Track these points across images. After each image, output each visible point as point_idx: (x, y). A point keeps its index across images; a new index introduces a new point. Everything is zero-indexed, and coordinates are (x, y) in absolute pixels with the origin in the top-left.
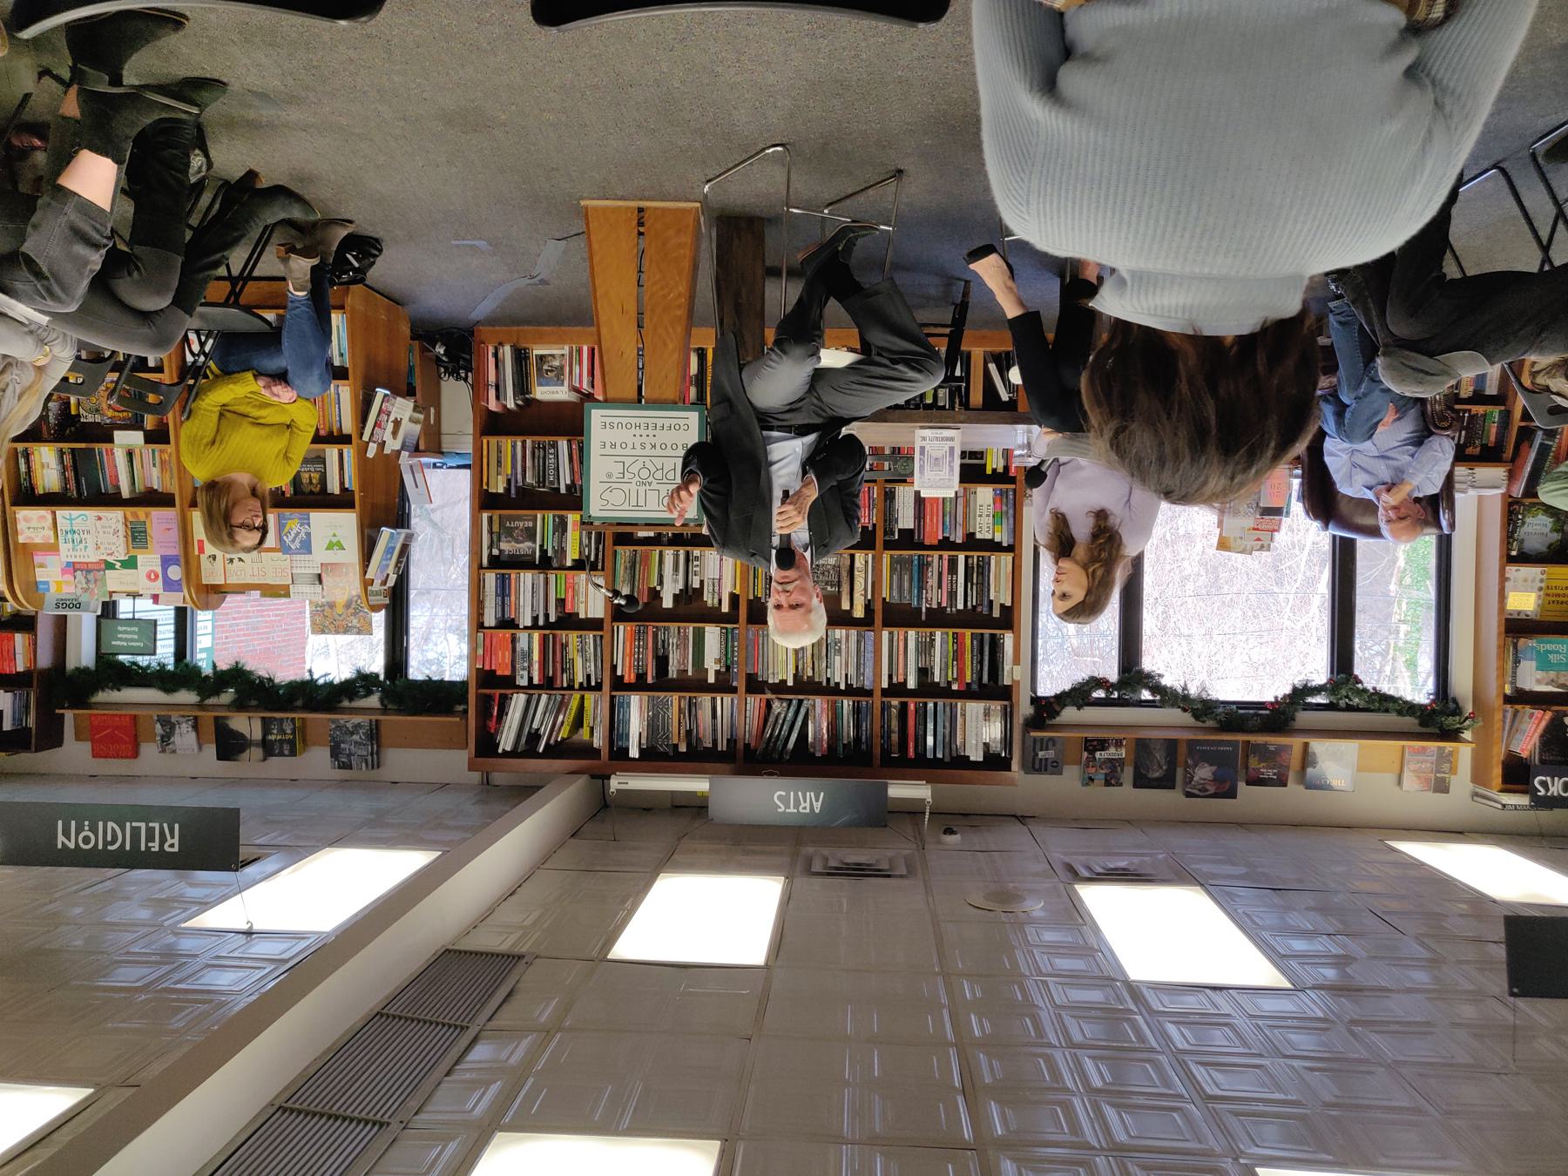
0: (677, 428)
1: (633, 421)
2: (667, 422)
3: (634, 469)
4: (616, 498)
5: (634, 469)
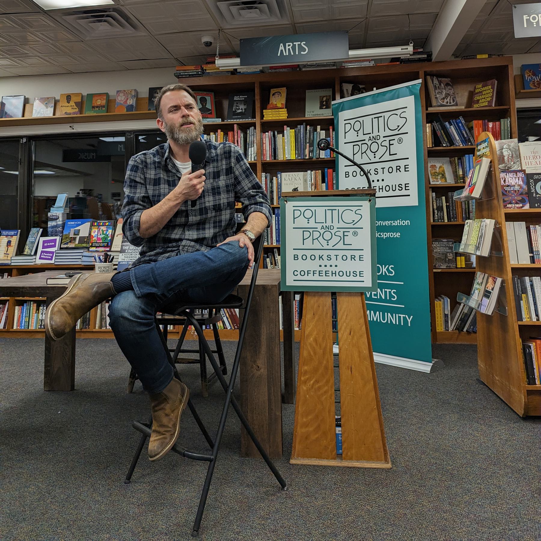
1: (338, 278)
2: (311, 277)
3: (335, 239)
4: (349, 216)
5: (335, 239)
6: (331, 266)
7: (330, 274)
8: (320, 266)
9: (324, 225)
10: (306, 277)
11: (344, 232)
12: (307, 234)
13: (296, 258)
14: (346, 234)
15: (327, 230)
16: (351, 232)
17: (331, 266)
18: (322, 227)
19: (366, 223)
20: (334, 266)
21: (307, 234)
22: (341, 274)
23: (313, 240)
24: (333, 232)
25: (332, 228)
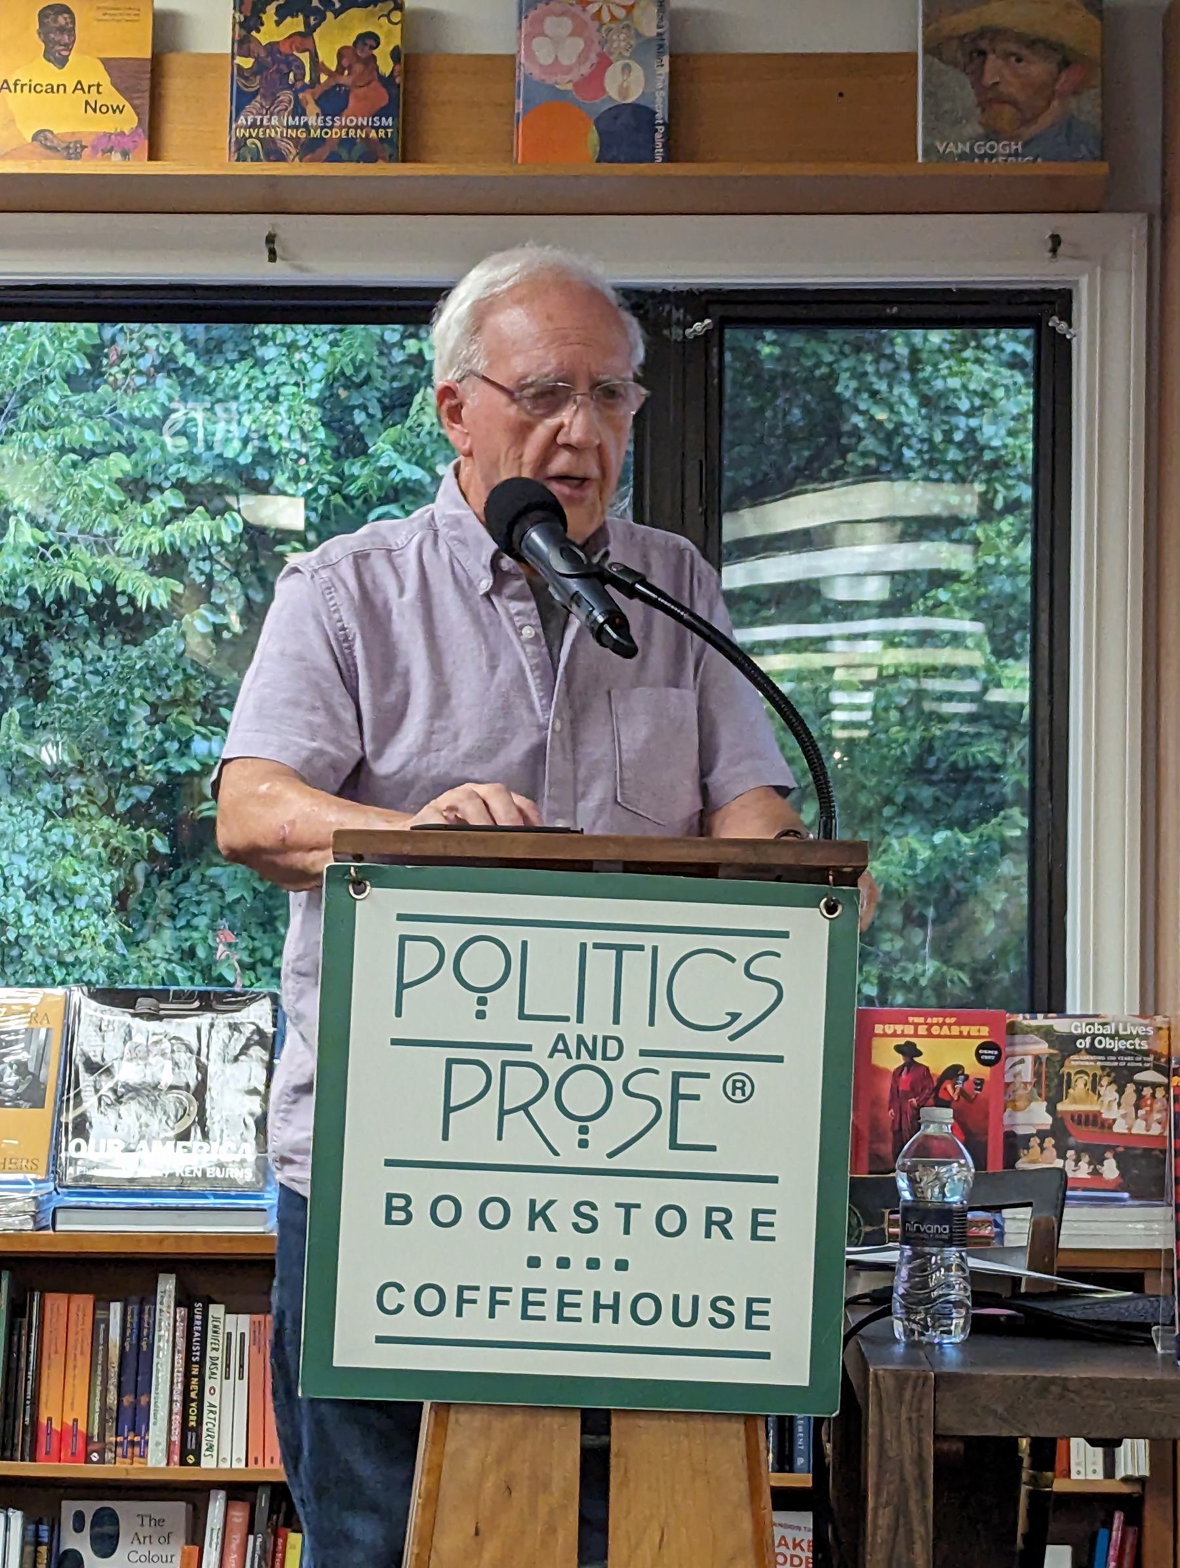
0: (431, 1298)
1: (627, 1332)
2: (475, 1323)
3: (629, 1115)
4: (712, 989)
5: (629, 1115)
6: (593, 1264)
7: (586, 1311)
8: (534, 1262)
9: (571, 1031)
10: (446, 1325)
11: (677, 1076)
12: (467, 1081)
13: (398, 1216)
14: (685, 1086)
15: (585, 1059)
16: (717, 1080)
17: (593, 1264)
18: (560, 1046)
19: (800, 1033)
20: (608, 1264)
21: (467, 1081)
22: (646, 1309)
23: (503, 1113)
24: (617, 1071)
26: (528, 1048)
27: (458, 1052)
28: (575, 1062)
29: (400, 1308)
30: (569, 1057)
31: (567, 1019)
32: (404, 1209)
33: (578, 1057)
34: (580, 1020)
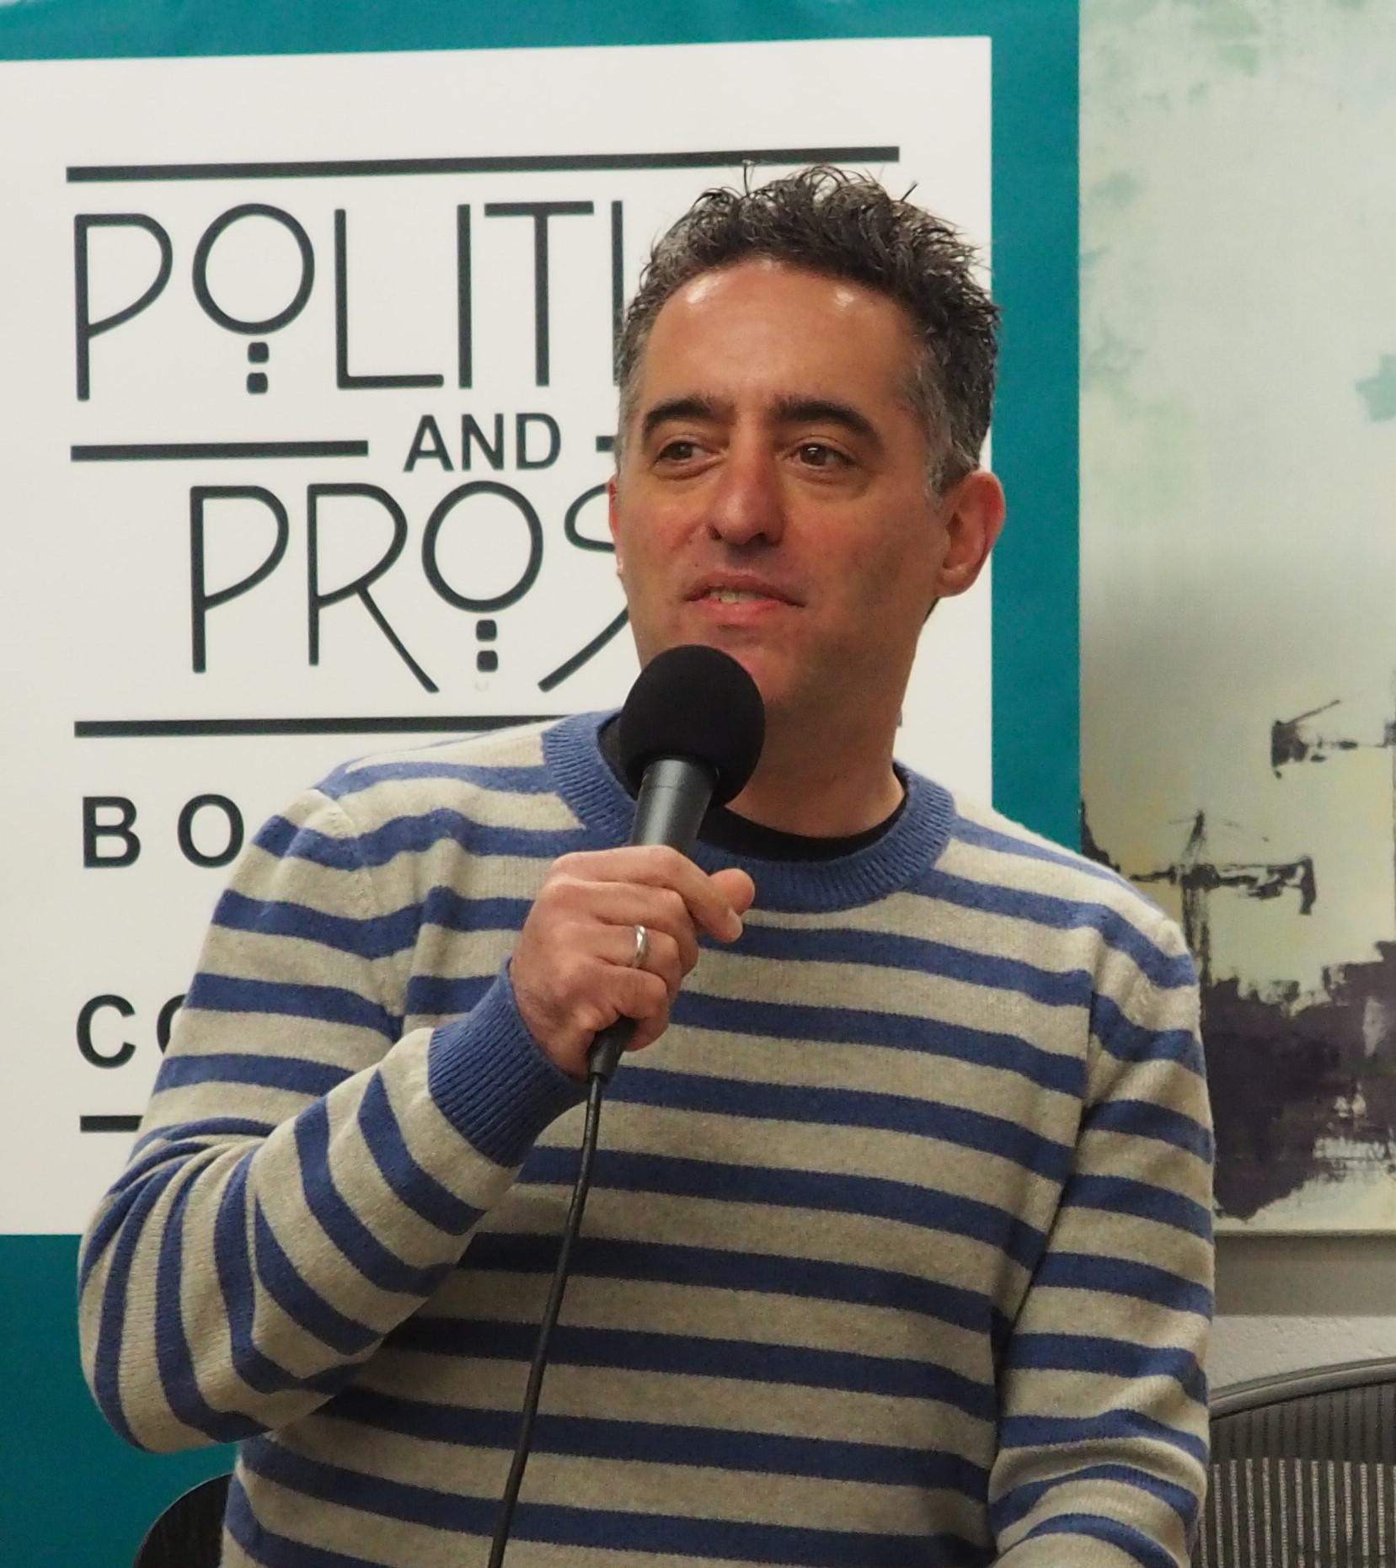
9: (449, 406)
12: (239, 536)
15: (482, 469)
18: (426, 443)
23: (317, 602)
24: (550, 494)
25: (538, 441)
26: (358, 448)
27: (212, 465)
28: (459, 477)
29: (127, 1051)
30: (447, 465)
31: (435, 381)
32: (122, 830)
33: (467, 464)
34: (465, 380)
